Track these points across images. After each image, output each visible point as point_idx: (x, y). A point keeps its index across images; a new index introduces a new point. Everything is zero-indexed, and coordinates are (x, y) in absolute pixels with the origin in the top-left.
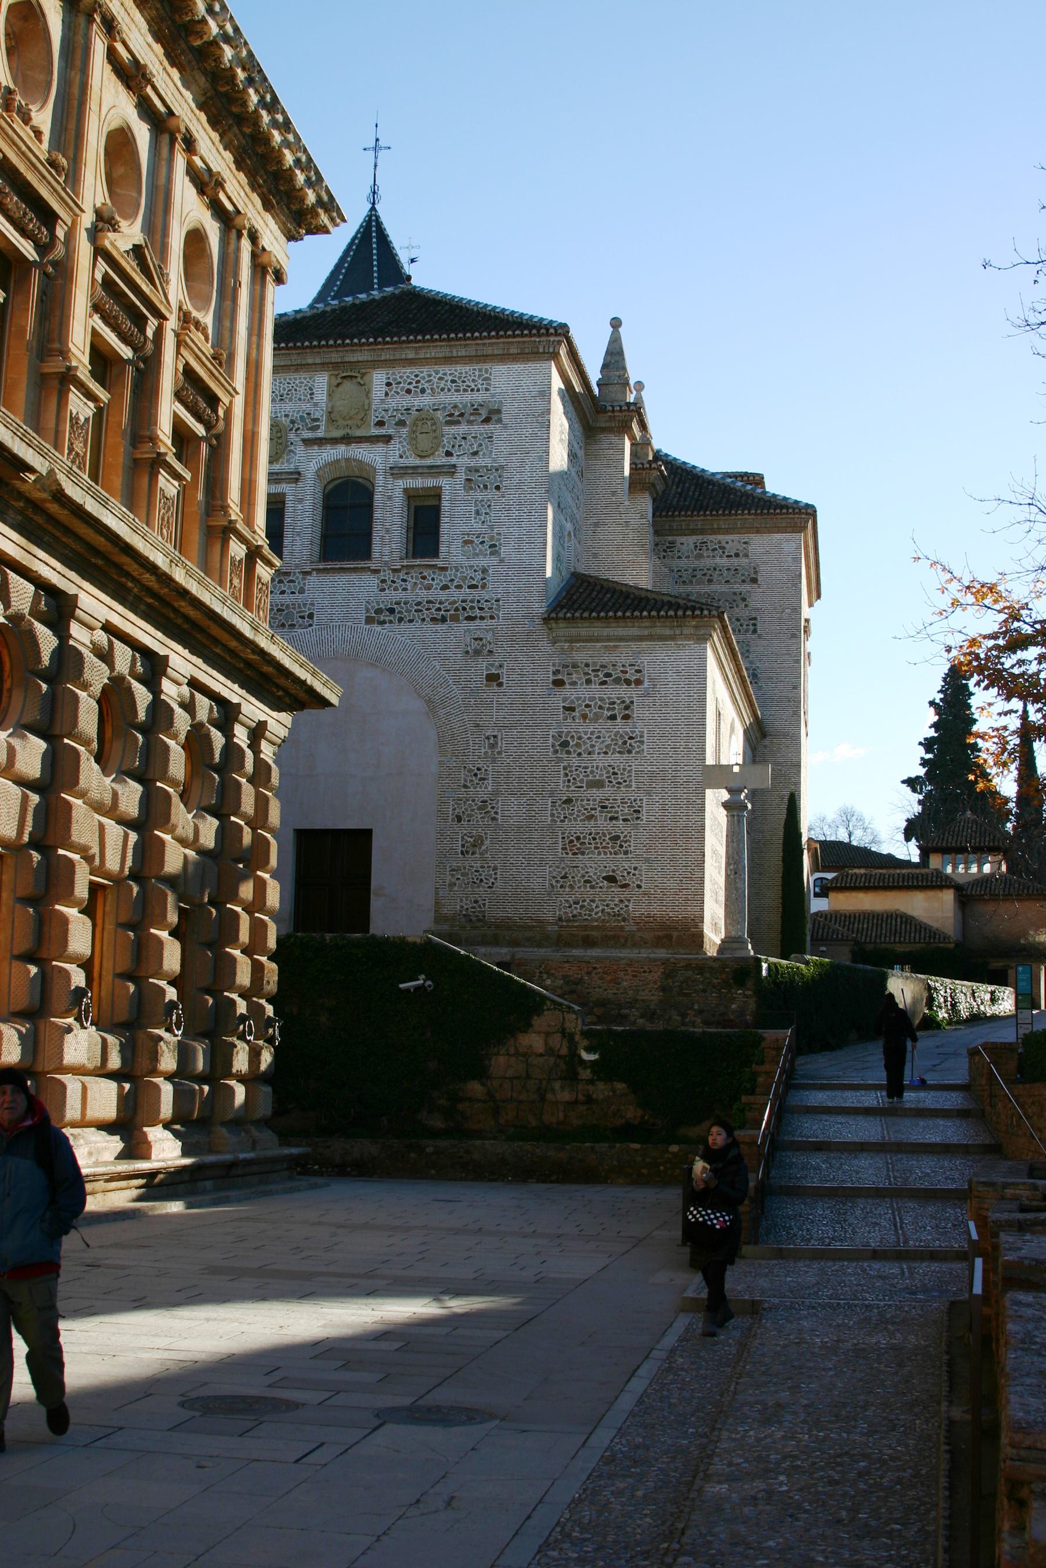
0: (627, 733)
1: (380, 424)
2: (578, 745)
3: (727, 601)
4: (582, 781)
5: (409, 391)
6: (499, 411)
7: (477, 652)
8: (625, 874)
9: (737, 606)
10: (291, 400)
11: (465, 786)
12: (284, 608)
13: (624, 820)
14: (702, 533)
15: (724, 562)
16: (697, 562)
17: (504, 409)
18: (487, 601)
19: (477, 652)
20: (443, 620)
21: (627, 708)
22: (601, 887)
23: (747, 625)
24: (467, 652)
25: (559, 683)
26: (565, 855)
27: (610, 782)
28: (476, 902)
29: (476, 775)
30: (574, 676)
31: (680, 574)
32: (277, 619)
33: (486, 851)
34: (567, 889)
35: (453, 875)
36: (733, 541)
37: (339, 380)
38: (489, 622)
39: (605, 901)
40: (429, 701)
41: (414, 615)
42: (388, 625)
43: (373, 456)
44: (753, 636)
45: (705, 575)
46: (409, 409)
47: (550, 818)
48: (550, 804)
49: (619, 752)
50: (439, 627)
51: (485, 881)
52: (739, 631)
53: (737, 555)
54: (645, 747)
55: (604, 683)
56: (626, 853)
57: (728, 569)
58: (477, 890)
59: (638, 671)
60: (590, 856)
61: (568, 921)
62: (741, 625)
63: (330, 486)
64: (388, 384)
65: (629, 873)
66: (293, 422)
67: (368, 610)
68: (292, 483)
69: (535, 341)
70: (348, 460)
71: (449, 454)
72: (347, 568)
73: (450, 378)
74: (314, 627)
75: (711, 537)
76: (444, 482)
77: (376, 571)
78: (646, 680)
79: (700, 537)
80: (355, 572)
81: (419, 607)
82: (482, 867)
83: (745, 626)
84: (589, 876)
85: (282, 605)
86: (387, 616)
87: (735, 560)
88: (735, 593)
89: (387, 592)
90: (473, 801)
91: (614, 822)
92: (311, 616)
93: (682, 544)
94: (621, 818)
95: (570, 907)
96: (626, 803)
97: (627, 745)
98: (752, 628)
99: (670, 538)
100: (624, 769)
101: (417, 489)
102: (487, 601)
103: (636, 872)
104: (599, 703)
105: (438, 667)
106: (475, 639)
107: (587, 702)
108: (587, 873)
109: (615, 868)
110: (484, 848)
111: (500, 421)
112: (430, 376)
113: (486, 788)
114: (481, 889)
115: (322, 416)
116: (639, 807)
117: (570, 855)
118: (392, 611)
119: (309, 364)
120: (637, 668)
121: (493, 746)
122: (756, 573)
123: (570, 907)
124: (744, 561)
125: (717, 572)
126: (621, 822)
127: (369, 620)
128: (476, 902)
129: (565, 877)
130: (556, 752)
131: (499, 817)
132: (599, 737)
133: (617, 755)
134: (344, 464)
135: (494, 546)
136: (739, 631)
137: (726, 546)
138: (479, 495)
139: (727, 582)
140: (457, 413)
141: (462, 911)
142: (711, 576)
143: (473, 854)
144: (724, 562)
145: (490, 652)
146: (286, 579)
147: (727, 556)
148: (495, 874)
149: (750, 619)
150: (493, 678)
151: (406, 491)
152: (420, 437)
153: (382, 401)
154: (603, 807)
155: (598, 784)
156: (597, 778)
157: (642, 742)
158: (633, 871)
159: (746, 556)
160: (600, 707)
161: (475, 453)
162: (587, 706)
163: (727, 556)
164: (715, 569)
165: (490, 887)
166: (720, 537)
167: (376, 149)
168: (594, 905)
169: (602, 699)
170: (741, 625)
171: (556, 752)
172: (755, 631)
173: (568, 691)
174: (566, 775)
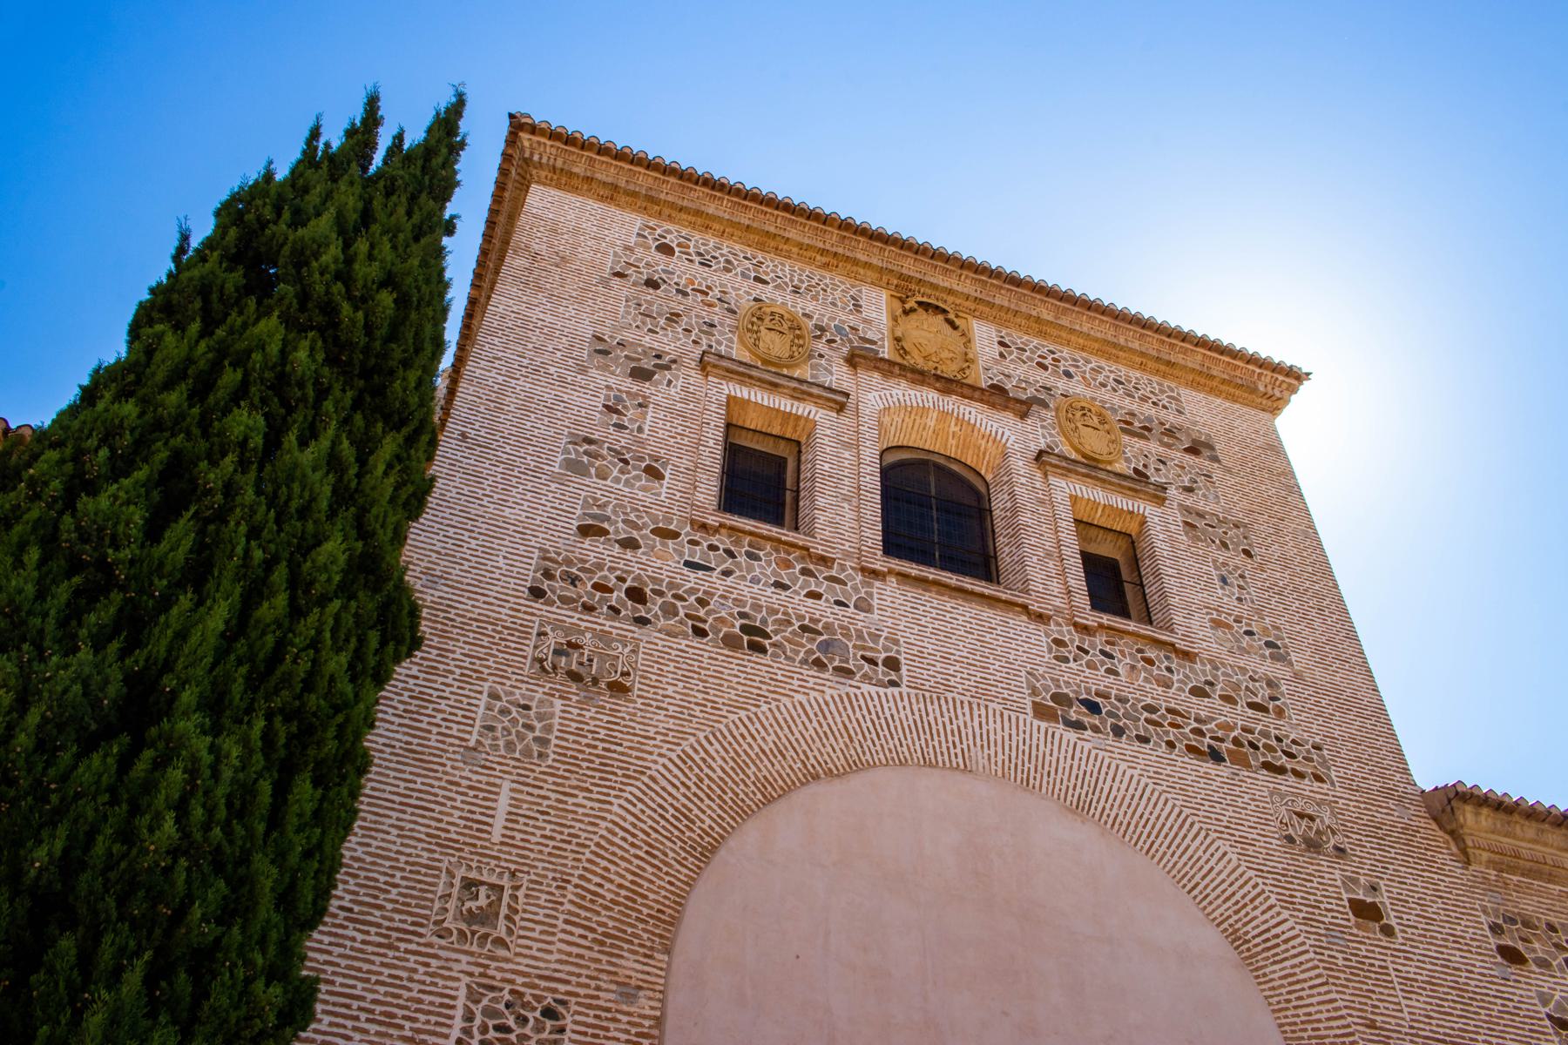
10: (815, 298)
12: (820, 627)
20: (1216, 756)
24: (1290, 839)
32: (803, 646)
37: (911, 304)
38: (1307, 785)
40: (1236, 938)
41: (1146, 730)
42: (1089, 732)
46: (1050, 389)
50: (1209, 767)
67: (1035, 692)
68: (831, 409)
69: (1254, 372)
70: (944, 415)
72: (972, 593)
73: (1112, 376)
74: (904, 689)
80: (991, 606)
81: (1154, 716)
86: (1084, 714)
89: (1072, 664)
101: (1096, 504)
105: (1234, 857)
106: (1301, 816)
115: (882, 339)
119: (856, 262)
127: (1041, 712)
134: (932, 423)
145: (1340, 851)
146: (822, 572)
152: (1084, 431)
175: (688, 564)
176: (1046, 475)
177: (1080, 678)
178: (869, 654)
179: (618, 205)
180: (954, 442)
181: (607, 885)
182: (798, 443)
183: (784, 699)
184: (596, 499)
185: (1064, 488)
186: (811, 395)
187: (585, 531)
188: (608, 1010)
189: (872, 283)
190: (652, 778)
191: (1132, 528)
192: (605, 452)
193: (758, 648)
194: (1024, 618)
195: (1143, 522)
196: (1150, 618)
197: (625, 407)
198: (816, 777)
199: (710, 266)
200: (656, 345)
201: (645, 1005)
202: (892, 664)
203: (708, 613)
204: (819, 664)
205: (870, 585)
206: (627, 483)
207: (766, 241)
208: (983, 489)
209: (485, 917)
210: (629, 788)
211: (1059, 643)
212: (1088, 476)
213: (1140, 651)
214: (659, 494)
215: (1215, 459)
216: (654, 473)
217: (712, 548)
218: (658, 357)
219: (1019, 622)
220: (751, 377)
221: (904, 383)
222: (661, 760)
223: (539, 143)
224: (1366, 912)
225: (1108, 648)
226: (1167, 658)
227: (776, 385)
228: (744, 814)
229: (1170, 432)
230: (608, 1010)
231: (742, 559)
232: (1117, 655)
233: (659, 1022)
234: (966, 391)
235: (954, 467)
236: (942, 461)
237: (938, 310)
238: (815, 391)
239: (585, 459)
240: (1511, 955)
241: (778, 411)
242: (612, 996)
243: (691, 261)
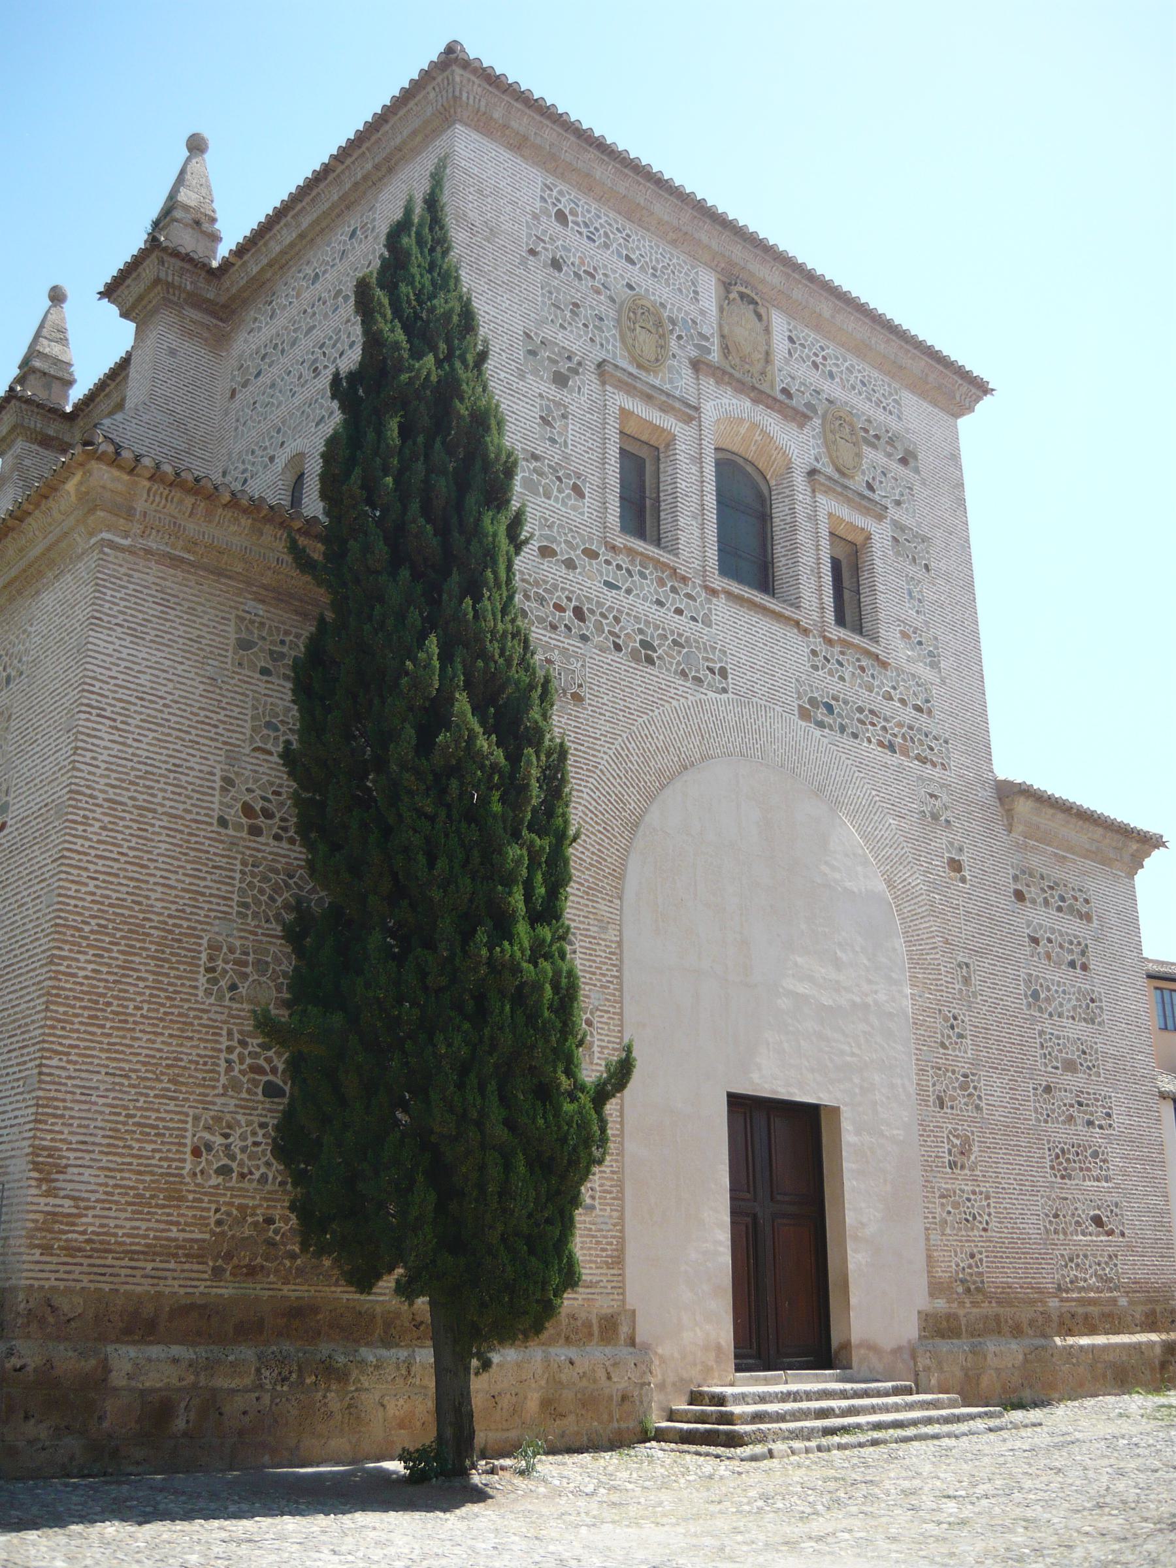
11: (943, 1045)
26: (1053, 1179)
29: (952, 1027)
34: (1061, 1237)
35: (943, 1205)
51: (978, 1218)
58: (970, 1233)
60: (1077, 1182)
65: (1112, 1211)
70: (754, 426)
82: (974, 1193)
84: (1079, 1216)
85: (680, 635)
90: (954, 1072)
110: (973, 1158)
113: (966, 1052)
114: (976, 1233)
121: (966, 981)
123: (1066, 1266)
128: (972, 1256)
129: (1056, 1216)
134: (743, 431)
141: (957, 1273)
143: (962, 1167)
148: (989, 1205)
175: (607, 583)
176: (814, 491)
177: (826, 684)
178: (711, 665)
179: (522, 156)
180: (754, 449)
181: (587, 853)
182: (657, 449)
183: (667, 705)
184: (546, 520)
185: (827, 504)
186: (673, 408)
188: (595, 938)
189: (705, 264)
190: (601, 771)
191: (859, 539)
192: (546, 469)
193: (650, 661)
194: (796, 631)
195: (869, 538)
196: (861, 628)
197: (553, 418)
198: (686, 768)
199: (594, 241)
200: (566, 344)
201: (612, 935)
202: (723, 673)
203: (621, 629)
204: (684, 674)
205: (709, 601)
206: (564, 504)
207: (632, 212)
208: (766, 492)
210: (591, 780)
211: (814, 653)
212: (841, 494)
213: (858, 660)
214: (582, 514)
215: (917, 471)
216: (578, 491)
217: (619, 567)
218: (569, 358)
219: (792, 634)
220: (635, 388)
221: (729, 391)
222: (606, 757)
223: (469, 80)
224: (955, 865)
225: (841, 658)
226: (873, 666)
228: (651, 798)
229: (891, 442)
230: (595, 938)
231: (636, 578)
232: (845, 663)
233: (620, 944)
234: (770, 401)
235: (749, 469)
236: (741, 461)
237: (753, 302)
238: (677, 405)
239: (535, 477)
240: (1019, 896)
241: (651, 423)
242: (595, 929)
243: (580, 233)
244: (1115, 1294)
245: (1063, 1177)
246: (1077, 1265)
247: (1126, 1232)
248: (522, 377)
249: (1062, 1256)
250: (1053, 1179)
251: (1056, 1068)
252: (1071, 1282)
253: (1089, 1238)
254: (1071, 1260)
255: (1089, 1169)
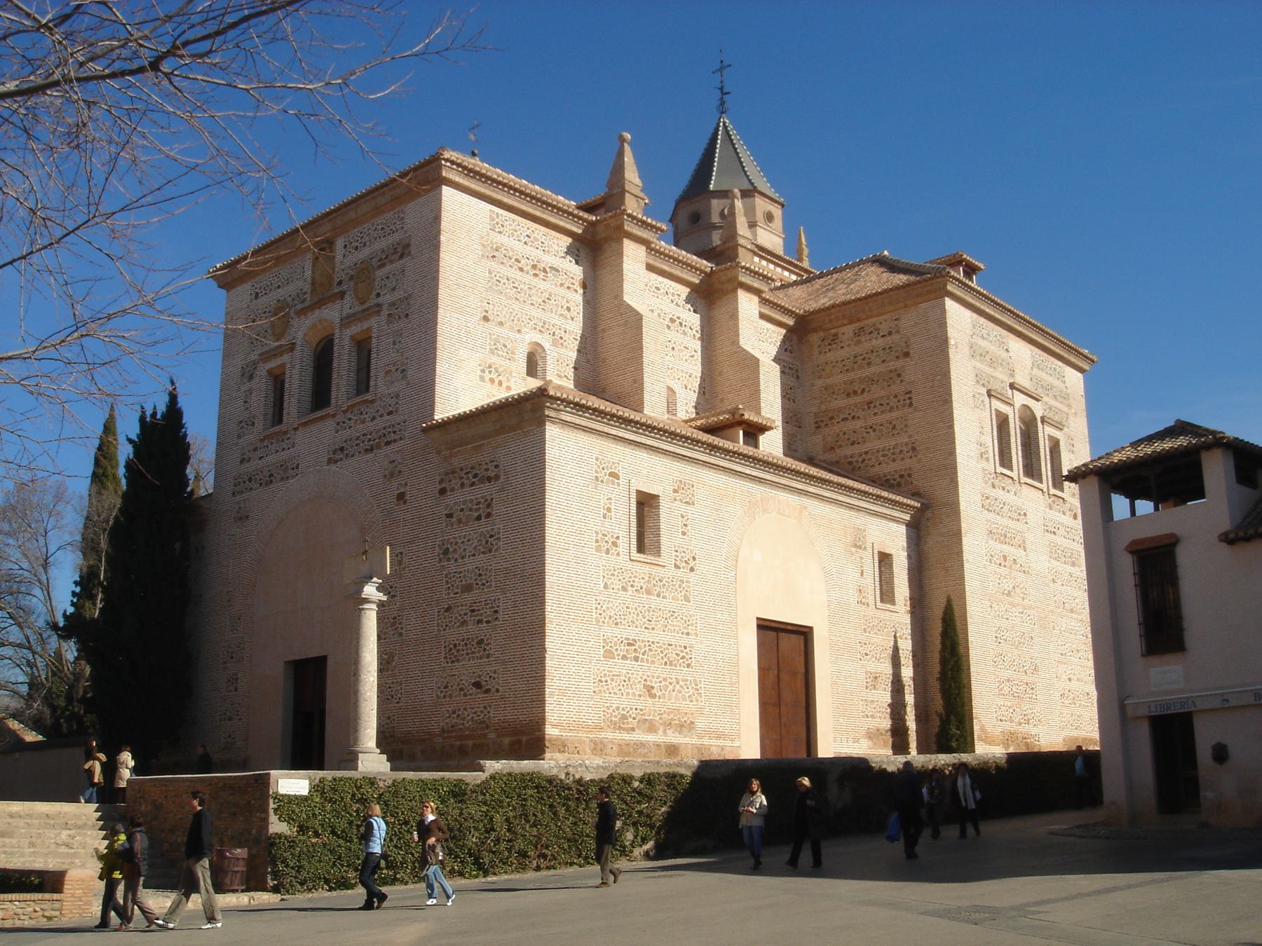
0: (488, 531)
1: (340, 283)
2: (455, 551)
3: (884, 380)
4: (458, 586)
5: (356, 248)
6: (408, 245)
7: (392, 475)
8: (488, 679)
9: (894, 383)
13: (488, 622)
14: (859, 320)
15: (878, 343)
16: (856, 348)
17: (413, 241)
18: (399, 424)
19: (392, 475)
20: (371, 450)
21: (489, 506)
22: (471, 695)
23: (904, 400)
25: (443, 492)
26: (446, 665)
27: (477, 584)
28: (389, 718)
30: (453, 481)
31: (844, 363)
33: (395, 666)
34: (448, 699)
36: (885, 321)
39: (472, 708)
43: (332, 313)
44: (910, 410)
45: (864, 359)
47: (436, 628)
48: (437, 614)
49: (483, 553)
50: (371, 455)
51: (395, 697)
52: (897, 407)
53: (890, 333)
54: (501, 543)
55: (473, 484)
56: (488, 656)
57: (884, 349)
59: (496, 467)
61: (448, 732)
62: (899, 401)
63: (320, 348)
64: (345, 247)
65: (490, 677)
66: (293, 300)
71: (378, 295)
73: (380, 227)
75: (866, 322)
76: (373, 322)
77: (334, 416)
78: (502, 474)
79: (857, 325)
82: (393, 683)
83: (902, 402)
84: (463, 684)
87: (889, 338)
88: (891, 371)
91: (480, 626)
92: (297, 467)
93: (843, 334)
94: (485, 620)
95: (449, 717)
96: (488, 604)
97: (488, 544)
98: (908, 401)
99: (833, 331)
100: (487, 569)
102: (399, 424)
103: (496, 676)
104: (470, 505)
107: (462, 506)
108: (461, 680)
109: (480, 673)
110: (394, 664)
111: (409, 254)
112: (368, 230)
114: (392, 705)
116: (498, 606)
117: (450, 665)
118: (342, 449)
120: (495, 463)
122: (908, 346)
124: (895, 337)
125: (875, 355)
126: (485, 625)
127: (330, 461)
129: (446, 687)
130: (440, 560)
131: (403, 631)
132: (469, 540)
133: (482, 555)
134: (319, 327)
135: (404, 370)
136: (897, 407)
137: (880, 326)
138: (395, 326)
139: (884, 361)
140: (384, 257)
142: (870, 359)
144: (878, 343)
145: (400, 472)
147: (882, 336)
149: (907, 393)
150: (401, 497)
151: (352, 338)
153: (342, 263)
154: (473, 611)
155: (468, 588)
156: (468, 582)
157: (498, 539)
158: (493, 675)
159: (898, 332)
160: (471, 510)
161: (394, 289)
162: (462, 510)
163: (882, 336)
164: (872, 351)
165: (398, 703)
166: (874, 320)
167: (721, 69)
168: (466, 713)
169: (471, 501)
170: (899, 401)
171: (440, 560)
172: (911, 405)
173: (450, 499)
174: (447, 582)
187: (242, 461)
193: (271, 482)
209: (229, 601)
216: (253, 424)
227: (275, 355)
244: (486, 731)
245: (453, 662)
246: (458, 716)
247: (500, 689)
248: (239, 389)
249: (447, 711)
250: (446, 665)
251: (457, 593)
252: (452, 726)
253: (468, 697)
254: (454, 712)
255: (474, 653)
